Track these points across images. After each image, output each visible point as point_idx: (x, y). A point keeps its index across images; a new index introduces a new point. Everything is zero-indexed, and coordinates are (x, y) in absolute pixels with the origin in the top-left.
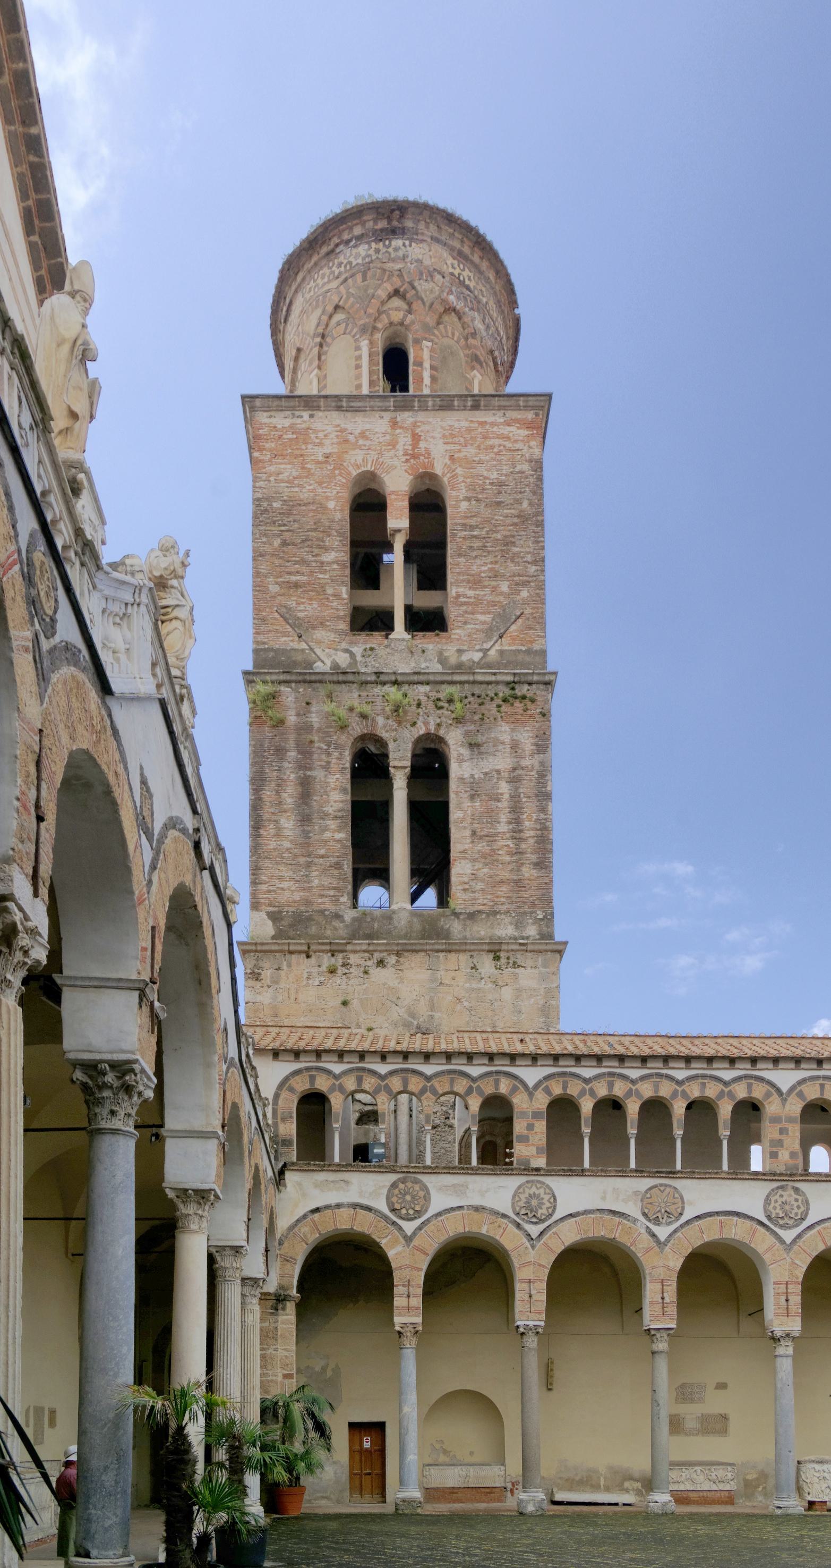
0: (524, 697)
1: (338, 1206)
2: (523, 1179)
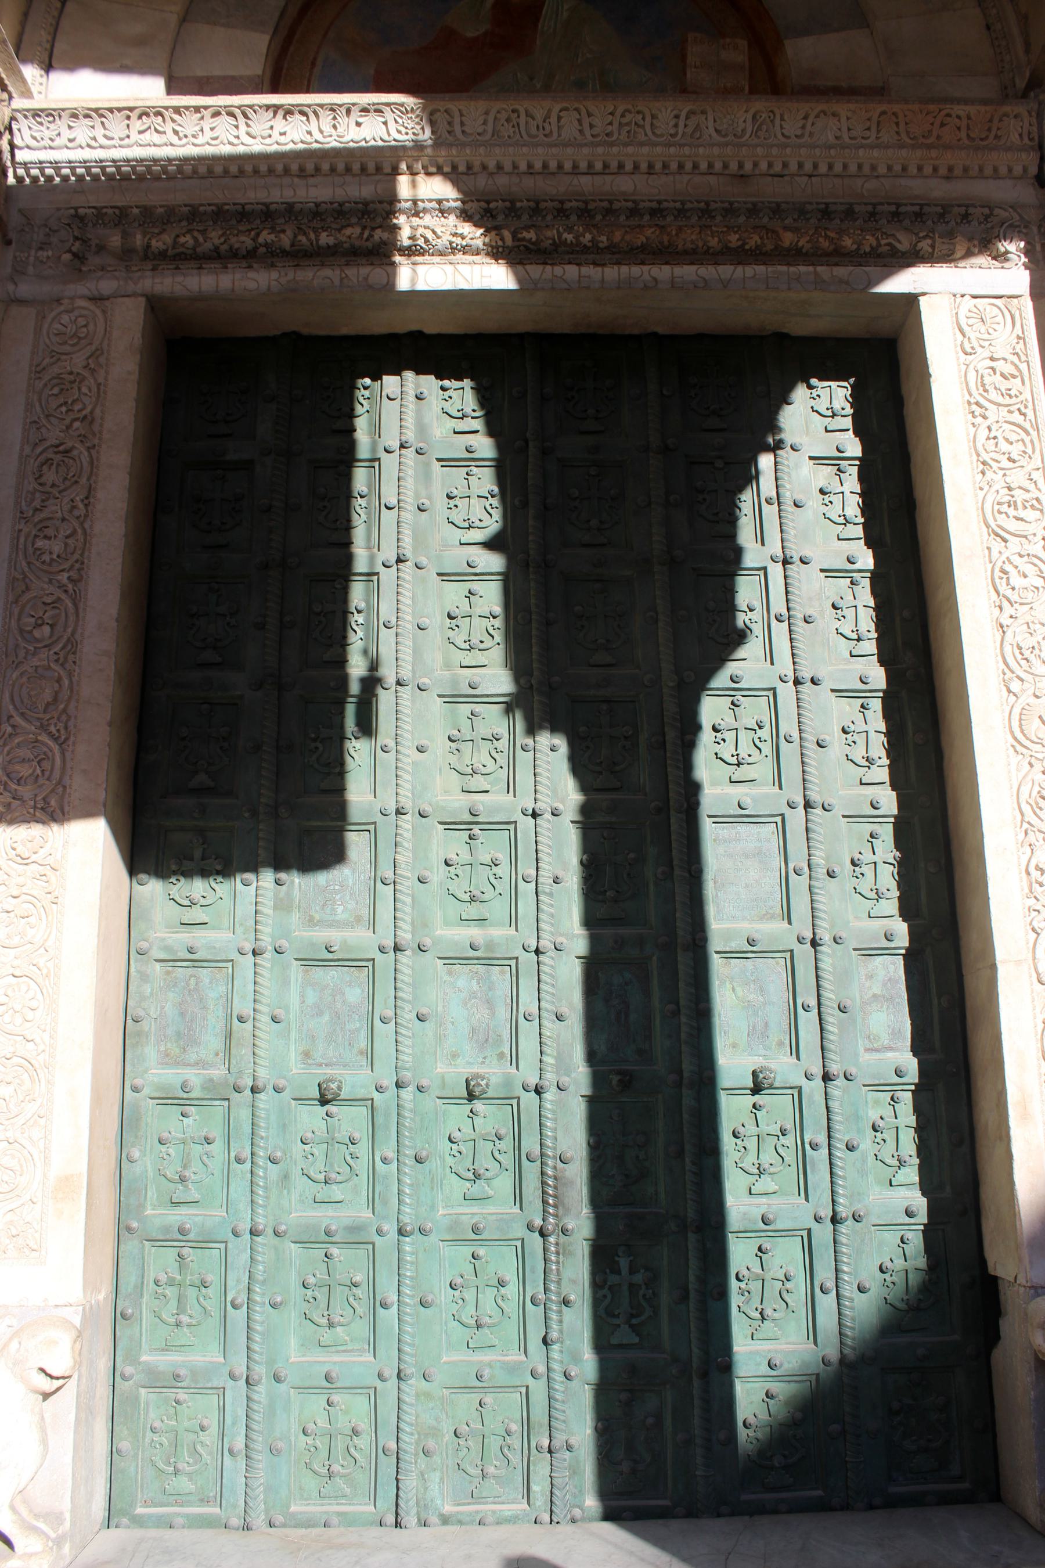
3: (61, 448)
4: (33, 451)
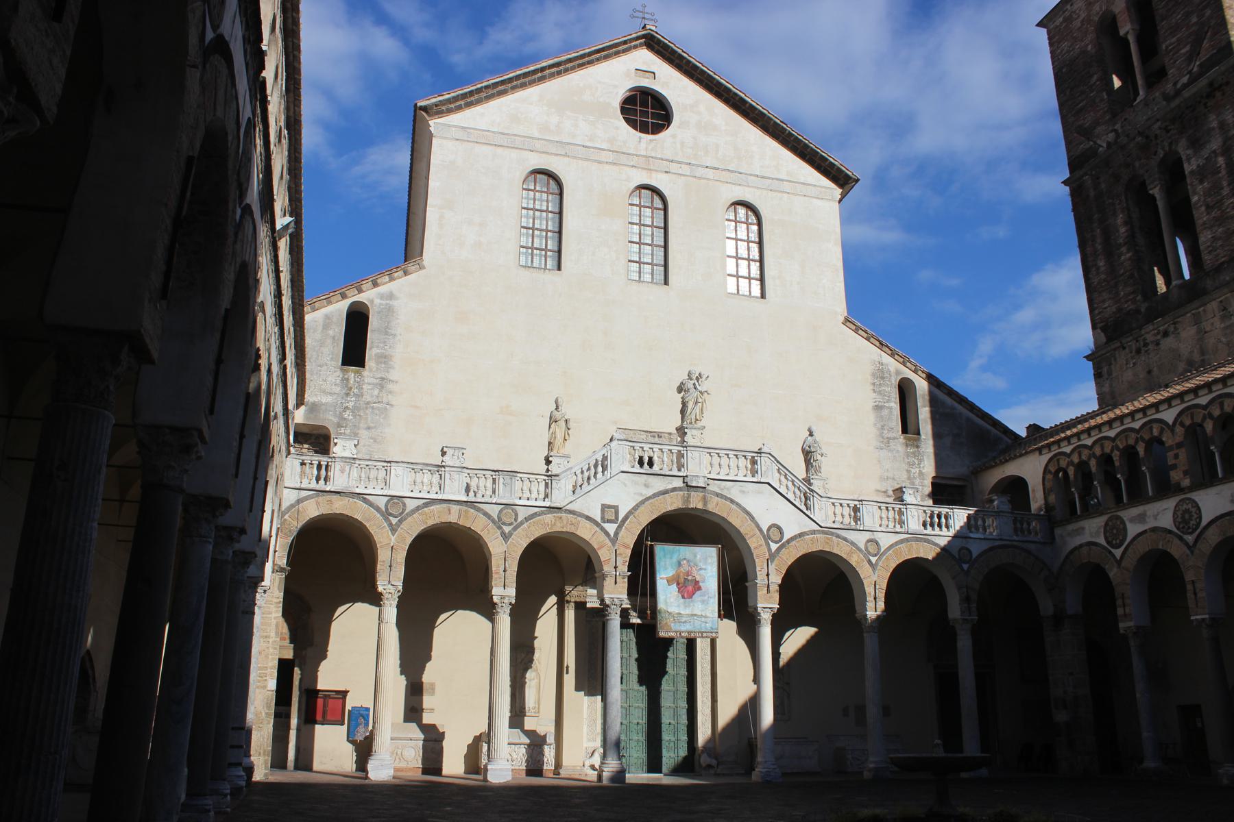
0: (1221, 86)
1: (1081, 546)
2: (1178, 499)
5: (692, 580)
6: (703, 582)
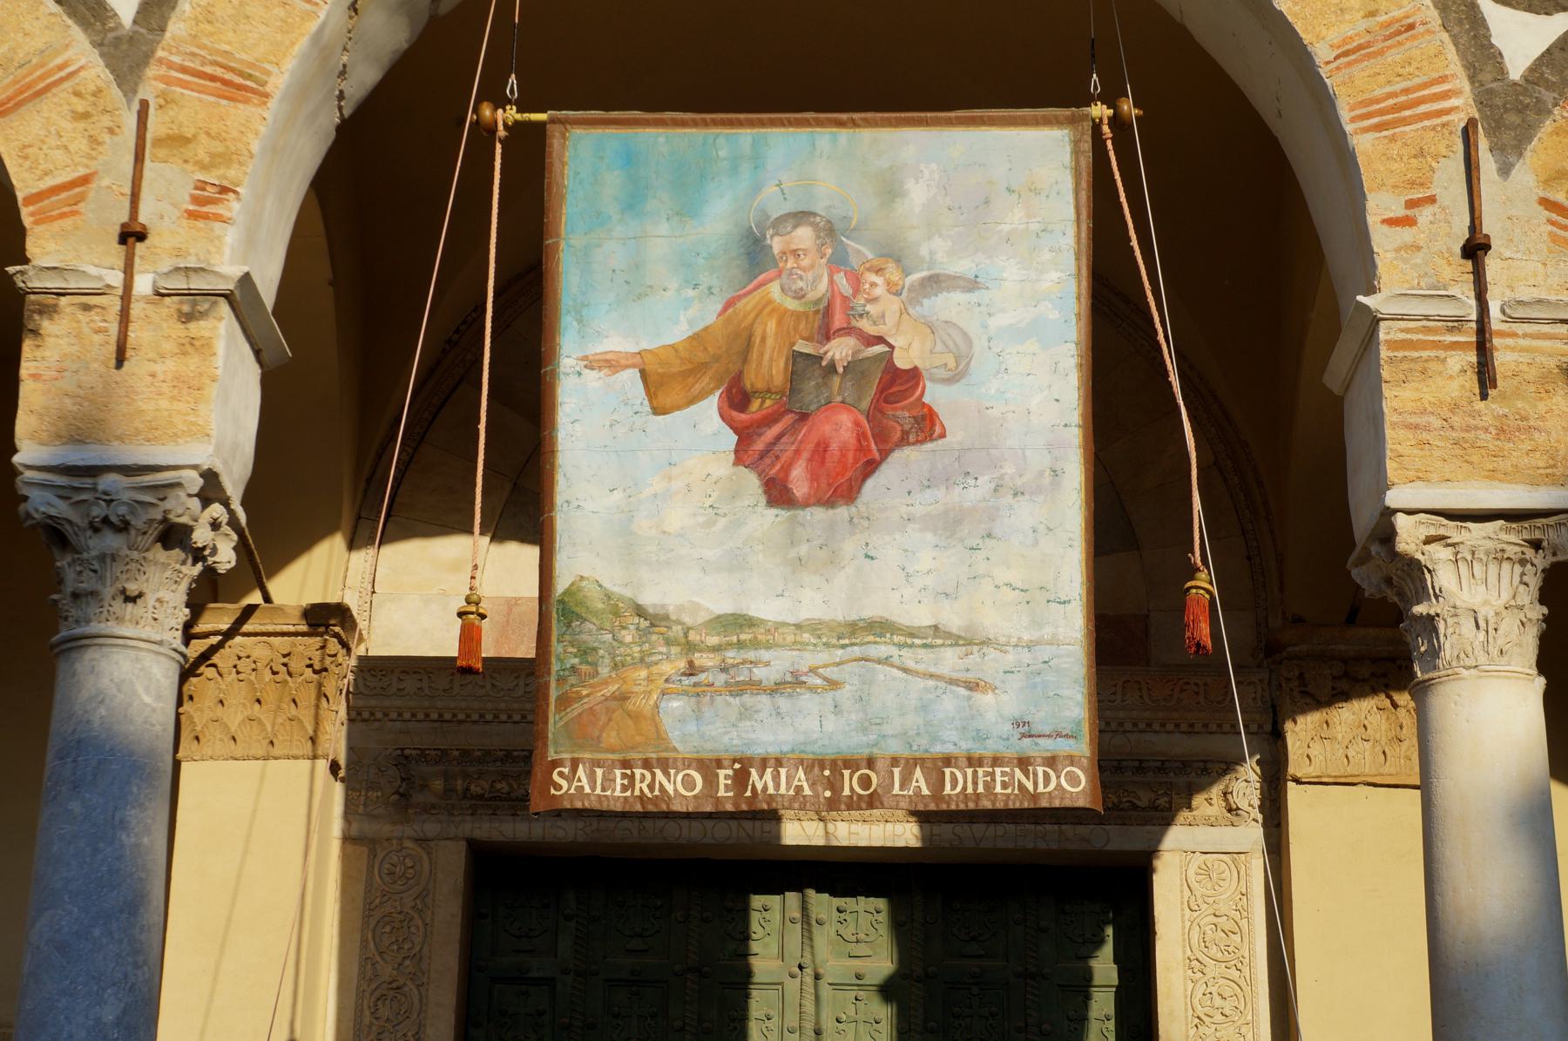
3: (394, 985)
4: (369, 986)
5: (855, 368)
6: (955, 377)
